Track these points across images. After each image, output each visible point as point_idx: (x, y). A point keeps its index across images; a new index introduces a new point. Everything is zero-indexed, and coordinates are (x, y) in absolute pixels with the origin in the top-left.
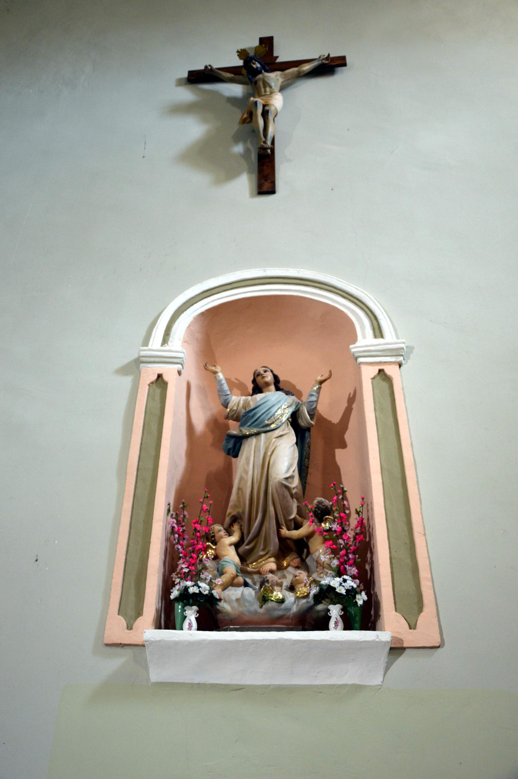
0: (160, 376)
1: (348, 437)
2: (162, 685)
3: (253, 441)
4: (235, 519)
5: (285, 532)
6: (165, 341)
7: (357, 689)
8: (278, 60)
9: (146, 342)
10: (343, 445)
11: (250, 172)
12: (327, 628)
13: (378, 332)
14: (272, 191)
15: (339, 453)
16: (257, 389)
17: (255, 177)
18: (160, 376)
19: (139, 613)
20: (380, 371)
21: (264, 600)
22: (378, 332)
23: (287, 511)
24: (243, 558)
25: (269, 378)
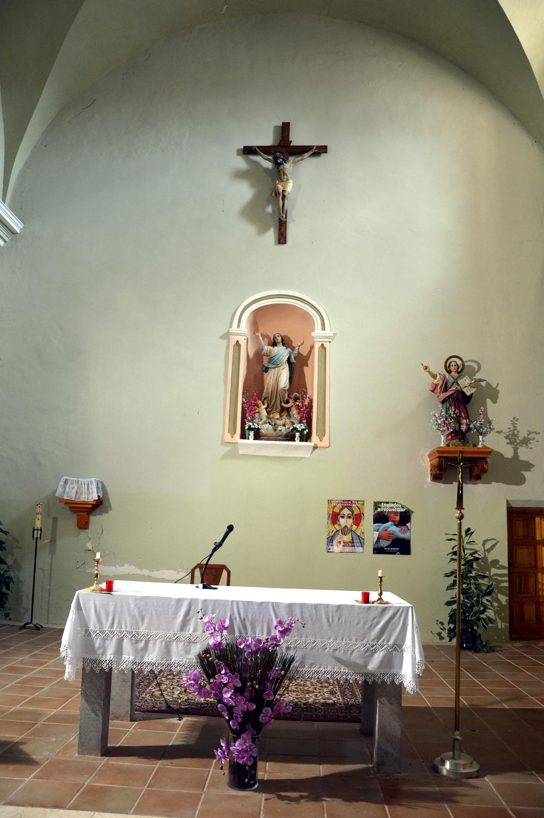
1: (309, 362)
3: (273, 370)
4: (265, 398)
5: (283, 404)
6: (238, 327)
7: (302, 458)
8: (292, 144)
9: (231, 326)
10: (307, 366)
11: (274, 228)
12: (294, 441)
13: (323, 328)
14: (285, 242)
15: (305, 368)
16: (274, 344)
17: (277, 231)
19: (235, 433)
21: (275, 430)
22: (323, 328)
23: (284, 397)
24: (268, 413)
25: (279, 339)
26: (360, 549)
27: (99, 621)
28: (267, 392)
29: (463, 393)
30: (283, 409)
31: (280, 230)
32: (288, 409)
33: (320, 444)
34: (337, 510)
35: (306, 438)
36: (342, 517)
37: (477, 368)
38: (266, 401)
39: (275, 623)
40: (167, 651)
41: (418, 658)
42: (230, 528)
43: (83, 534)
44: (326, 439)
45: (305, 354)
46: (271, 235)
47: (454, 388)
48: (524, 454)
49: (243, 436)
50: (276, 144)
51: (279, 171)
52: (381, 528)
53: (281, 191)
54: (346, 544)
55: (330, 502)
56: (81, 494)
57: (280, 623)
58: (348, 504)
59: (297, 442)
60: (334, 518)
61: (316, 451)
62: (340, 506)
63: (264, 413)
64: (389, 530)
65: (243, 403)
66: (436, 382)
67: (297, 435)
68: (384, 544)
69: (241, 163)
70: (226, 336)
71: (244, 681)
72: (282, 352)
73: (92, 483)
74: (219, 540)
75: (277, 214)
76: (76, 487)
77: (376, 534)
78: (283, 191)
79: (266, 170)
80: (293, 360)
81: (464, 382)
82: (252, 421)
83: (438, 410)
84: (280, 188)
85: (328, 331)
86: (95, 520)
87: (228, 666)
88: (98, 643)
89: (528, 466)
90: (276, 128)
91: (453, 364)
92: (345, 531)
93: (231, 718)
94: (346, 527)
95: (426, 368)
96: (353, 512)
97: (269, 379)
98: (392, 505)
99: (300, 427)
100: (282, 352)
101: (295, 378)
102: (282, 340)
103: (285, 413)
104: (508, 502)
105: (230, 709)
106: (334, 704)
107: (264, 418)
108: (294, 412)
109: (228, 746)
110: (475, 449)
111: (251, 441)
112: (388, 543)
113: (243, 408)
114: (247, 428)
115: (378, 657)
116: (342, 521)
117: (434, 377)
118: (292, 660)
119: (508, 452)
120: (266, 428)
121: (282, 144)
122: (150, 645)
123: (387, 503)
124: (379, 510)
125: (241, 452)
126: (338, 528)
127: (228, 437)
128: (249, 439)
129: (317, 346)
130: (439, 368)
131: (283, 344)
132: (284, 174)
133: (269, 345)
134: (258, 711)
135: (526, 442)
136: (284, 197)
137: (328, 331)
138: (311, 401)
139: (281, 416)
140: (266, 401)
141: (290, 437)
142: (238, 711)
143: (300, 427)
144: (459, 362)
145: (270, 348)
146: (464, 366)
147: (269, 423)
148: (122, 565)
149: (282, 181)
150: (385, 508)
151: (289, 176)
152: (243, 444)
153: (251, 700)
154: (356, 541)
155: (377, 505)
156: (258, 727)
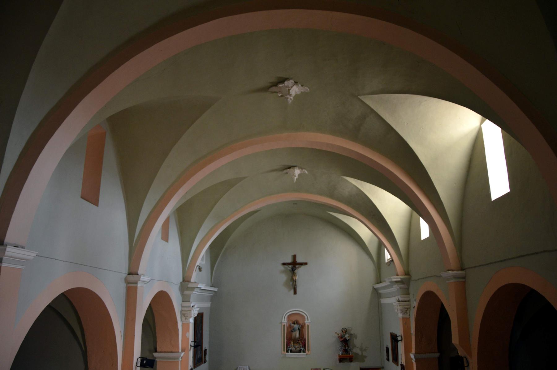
3: (294, 332)
6: (284, 320)
13: (308, 320)
16: (294, 323)
17: (294, 290)
22: (308, 320)
24: (294, 344)
25: (296, 322)
29: (346, 339)
30: (297, 343)
32: (299, 343)
35: (304, 352)
37: (351, 329)
38: (293, 341)
44: (310, 352)
45: (303, 325)
46: (292, 291)
47: (343, 338)
48: (365, 354)
49: (287, 352)
51: (294, 273)
53: (294, 280)
59: (302, 353)
63: (292, 344)
65: (287, 342)
66: (339, 336)
67: (302, 351)
69: (282, 268)
70: (281, 323)
72: (296, 326)
79: (290, 270)
80: (300, 328)
81: (347, 336)
82: (289, 347)
83: (340, 343)
84: (294, 278)
85: (309, 321)
89: (365, 357)
90: (292, 256)
91: (344, 330)
95: (336, 333)
97: (294, 334)
99: (303, 349)
102: (297, 322)
103: (298, 344)
104: (360, 367)
107: (293, 346)
108: (301, 343)
110: (349, 355)
111: (289, 353)
114: (288, 350)
117: (338, 335)
119: (360, 353)
120: (293, 349)
123: (327, 369)
125: (287, 356)
127: (283, 352)
128: (288, 352)
129: (306, 325)
130: (339, 331)
131: (297, 323)
132: (295, 274)
133: (293, 323)
135: (365, 350)
136: (295, 281)
138: (305, 339)
139: (297, 345)
140: (293, 341)
141: (300, 351)
143: (303, 349)
144: (345, 329)
146: (346, 329)
147: (294, 347)
149: (294, 276)
152: (288, 355)
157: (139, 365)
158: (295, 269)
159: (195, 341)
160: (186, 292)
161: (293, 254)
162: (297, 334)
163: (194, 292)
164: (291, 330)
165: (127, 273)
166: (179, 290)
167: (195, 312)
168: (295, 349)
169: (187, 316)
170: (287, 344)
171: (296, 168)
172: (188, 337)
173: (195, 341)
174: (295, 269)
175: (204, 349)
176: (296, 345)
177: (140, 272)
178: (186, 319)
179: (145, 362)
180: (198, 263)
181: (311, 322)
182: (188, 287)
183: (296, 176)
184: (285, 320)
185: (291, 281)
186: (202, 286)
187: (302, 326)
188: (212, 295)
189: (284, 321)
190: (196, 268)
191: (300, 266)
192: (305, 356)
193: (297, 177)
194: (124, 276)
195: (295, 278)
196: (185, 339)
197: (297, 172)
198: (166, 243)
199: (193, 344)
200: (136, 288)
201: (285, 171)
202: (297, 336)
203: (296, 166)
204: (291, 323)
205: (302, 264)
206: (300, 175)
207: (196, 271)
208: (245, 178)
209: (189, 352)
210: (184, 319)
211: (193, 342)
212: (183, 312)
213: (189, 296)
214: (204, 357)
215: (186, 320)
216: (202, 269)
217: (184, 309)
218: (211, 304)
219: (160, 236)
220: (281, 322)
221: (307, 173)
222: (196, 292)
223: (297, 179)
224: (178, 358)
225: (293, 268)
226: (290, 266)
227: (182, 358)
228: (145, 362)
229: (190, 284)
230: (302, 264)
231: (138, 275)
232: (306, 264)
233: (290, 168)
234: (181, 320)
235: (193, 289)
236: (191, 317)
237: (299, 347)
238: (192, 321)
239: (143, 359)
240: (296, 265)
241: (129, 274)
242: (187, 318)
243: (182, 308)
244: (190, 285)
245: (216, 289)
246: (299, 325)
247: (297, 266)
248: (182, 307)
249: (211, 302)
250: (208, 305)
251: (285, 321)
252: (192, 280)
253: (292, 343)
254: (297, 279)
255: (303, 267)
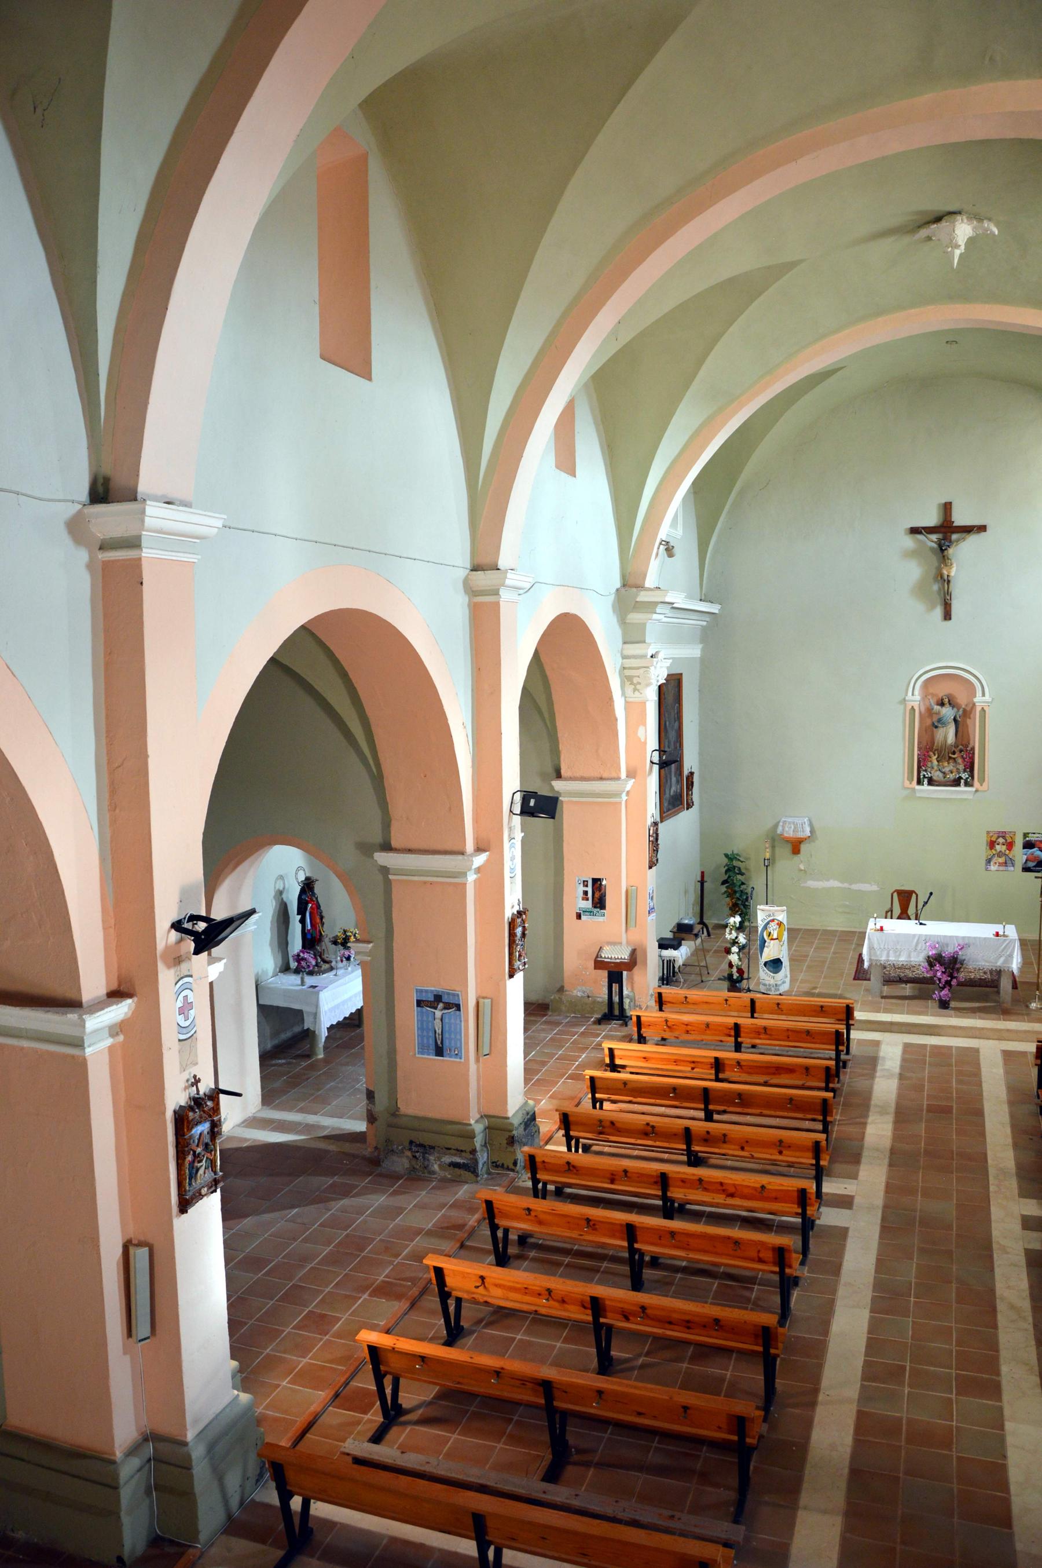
0: (913, 707)
1: (972, 716)
2: (920, 797)
3: (942, 729)
5: (950, 755)
6: (913, 695)
7: (966, 799)
8: (954, 525)
11: (941, 605)
13: (984, 695)
16: (942, 704)
17: (943, 607)
18: (913, 707)
19: (913, 780)
20: (983, 708)
22: (984, 695)
24: (938, 761)
25: (946, 701)
26: (1012, 868)
27: (879, 943)
28: (938, 743)
30: (950, 758)
31: (945, 608)
32: (954, 759)
33: (980, 788)
34: (994, 839)
35: (967, 784)
36: (998, 844)
38: (936, 752)
39: (957, 945)
40: (909, 956)
41: (1019, 961)
42: (931, 894)
43: (796, 858)
44: (985, 784)
45: (968, 709)
46: (939, 611)
49: (919, 782)
50: (939, 524)
51: (944, 556)
52: (1029, 853)
53: (946, 577)
54: (1000, 864)
55: (988, 832)
56: (797, 832)
57: (959, 945)
58: (1002, 835)
59: (962, 788)
60: (992, 845)
61: (977, 794)
62: (996, 836)
63: (935, 763)
64: (1035, 854)
65: (918, 755)
67: (962, 781)
68: (1031, 864)
69: (909, 542)
70: (904, 701)
71: (945, 968)
72: (948, 712)
73: (805, 823)
74: (926, 901)
75: (942, 593)
76: (793, 827)
77: (1025, 857)
78: (948, 576)
79: (932, 549)
82: (926, 771)
84: (945, 572)
85: (987, 698)
86: (803, 847)
87: (939, 963)
88: (878, 953)
90: (939, 505)
92: (1000, 854)
93: (940, 982)
94: (1000, 851)
96: (1006, 840)
97: (939, 734)
98: (1038, 835)
99: (965, 776)
100: (948, 714)
101: (960, 734)
102: (949, 701)
105: (940, 980)
106: (985, 979)
107: (936, 768)
108: (960, 760)
109: (939, 993)
111: (926, 787)
112: (1034, 864)
113: (918, 759)
114: (922, 777)
115: (1002, 960)
116: (998, 848)
118: (964, 960)
120: (937, 775)
121: (945, 525)
122: (902, 954)
123: (1034, 833)
124: (1027, 839)
125: (918, 795)
126: (994, 852)
127: (907, 783)
128: (923, 785)
129: (978, 709)
131: (950, 704)
132: (948, 559)
133: (937, 705)
134: (951, 980)
136: (949, 582)
137: (987, 698)
138: (973, 749)
139: (948, 763)
140: (936, 752)
141: (956, 783)
142: (943, 981)
145: (939, 707)
148: (828, 880)
149: (946, 566)
150: (1032, 838)
151: (953, 561)
153: (948, 976)
154: (1009, 862)
155: (1025, 835)
156: (950, 986)
157: (517, 809)
158: (947, 544)
159: (662, 749)
160: (634, 617)
161: (943, 501)
162: (948, 735)
163: (655, 616)
164: (932, 723)
165: (468, 566)
166: (614, 611)
167: (659, 674)
168: (941, 775)
169: (639, 683)
170: (919, 762)
171: (959, 218)
172: (643, 740)
173: (661, 751)
174: (947, 544)
175: (686, 772)
176: (946, 764)
177: (502, 563)
178: (635, 690)
179: (532, 803)
180: (663, 534)
181: (993, 699)
182: (637, 602)
183: (958, 246)
184: (917, 692)
185: (935, 579)
186: (680, 600)
187: (965, 711)
188: (705, 623)
189: (913, 698)
190: (658, 548)
191: (964, 535)
192: (970, 797)
193: (963, 247)
194: (462, 573)
195: (949, 572)
196: (636, 744)
197: (963, 230)
198: (570, 478)
199: (656, 758)
200: (497, 605)
201: (924, 233)
202: (951, 738)
203: (959, 213)
204: (933, 702)
205: (968, 530)
206: (971, 242)
207: (657, 554)
208: (793, 265)
209: (648, 780)
210: (629, 689)
211: (658, 752)
212: (627, 673)
213: (642, 627)
214: (687, 794)
215: (636, 692)
216: (676, 551)
217: (628, 663)
218: (703, 650)
219: (551, 459)
220: (904, 699)
221: (997, 233)
222: (660, 617)
223: (961, 255)
224: (618, 795)
225: (943, 541)
226: (934, 537)
227: (628, 793)
228: (532, 803)
229: (642, 593)
230: (968, 530)
231: (499, 569)
232: (982, 528)
233: (938, 219)
234: (623, 694)
235: (650, 607)
236: (649, 685)
237: (955, 770)
238: (651, 696)
239: (526, 796)
240: (953, 532)
241: (475, 569)
242: (638, 687)
243: (624, 660)
244: (643, 597)
245: (715, 608)
246: (955, 709)
247: (954, 537)
248: (624, 657)
249: (701, 643)
250: (695, 651)
251: (915, 698)
252: (649, 583)
253: (934, 758)
254: (952, 574)
255: (973, 539)
